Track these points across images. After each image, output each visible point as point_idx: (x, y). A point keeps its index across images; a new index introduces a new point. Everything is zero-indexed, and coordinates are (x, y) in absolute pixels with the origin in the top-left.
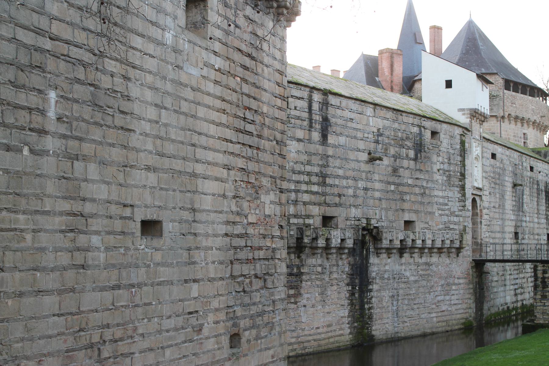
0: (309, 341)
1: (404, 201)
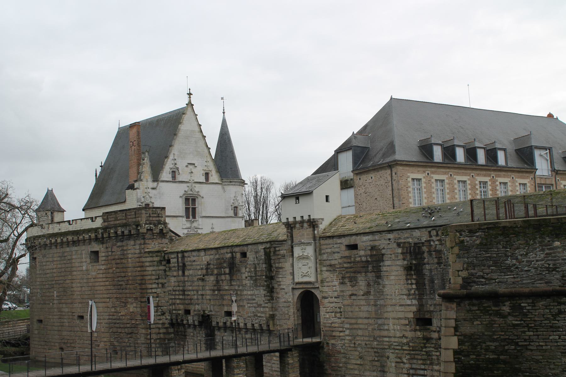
0: (189, 367)
1: (224, 299)
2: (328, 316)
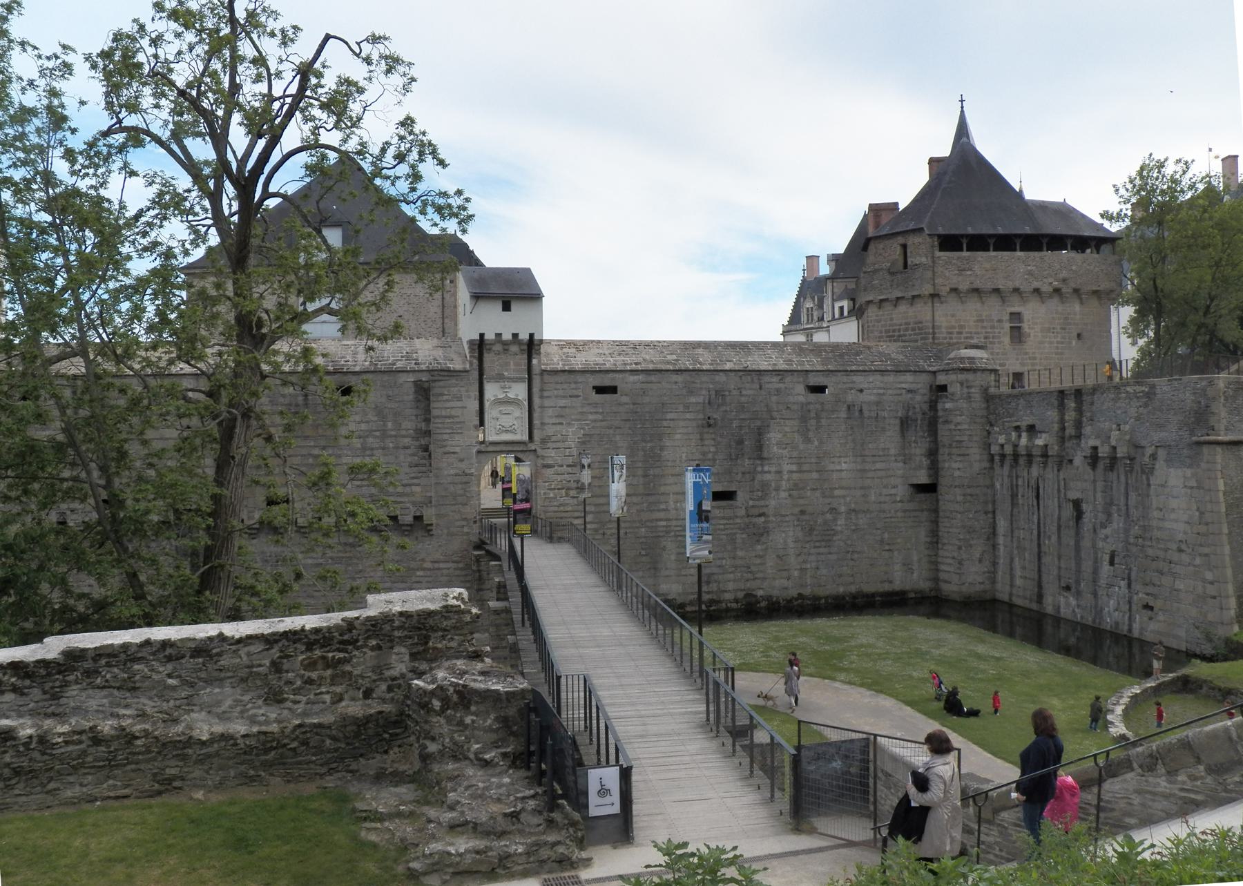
2: (552, 495)
